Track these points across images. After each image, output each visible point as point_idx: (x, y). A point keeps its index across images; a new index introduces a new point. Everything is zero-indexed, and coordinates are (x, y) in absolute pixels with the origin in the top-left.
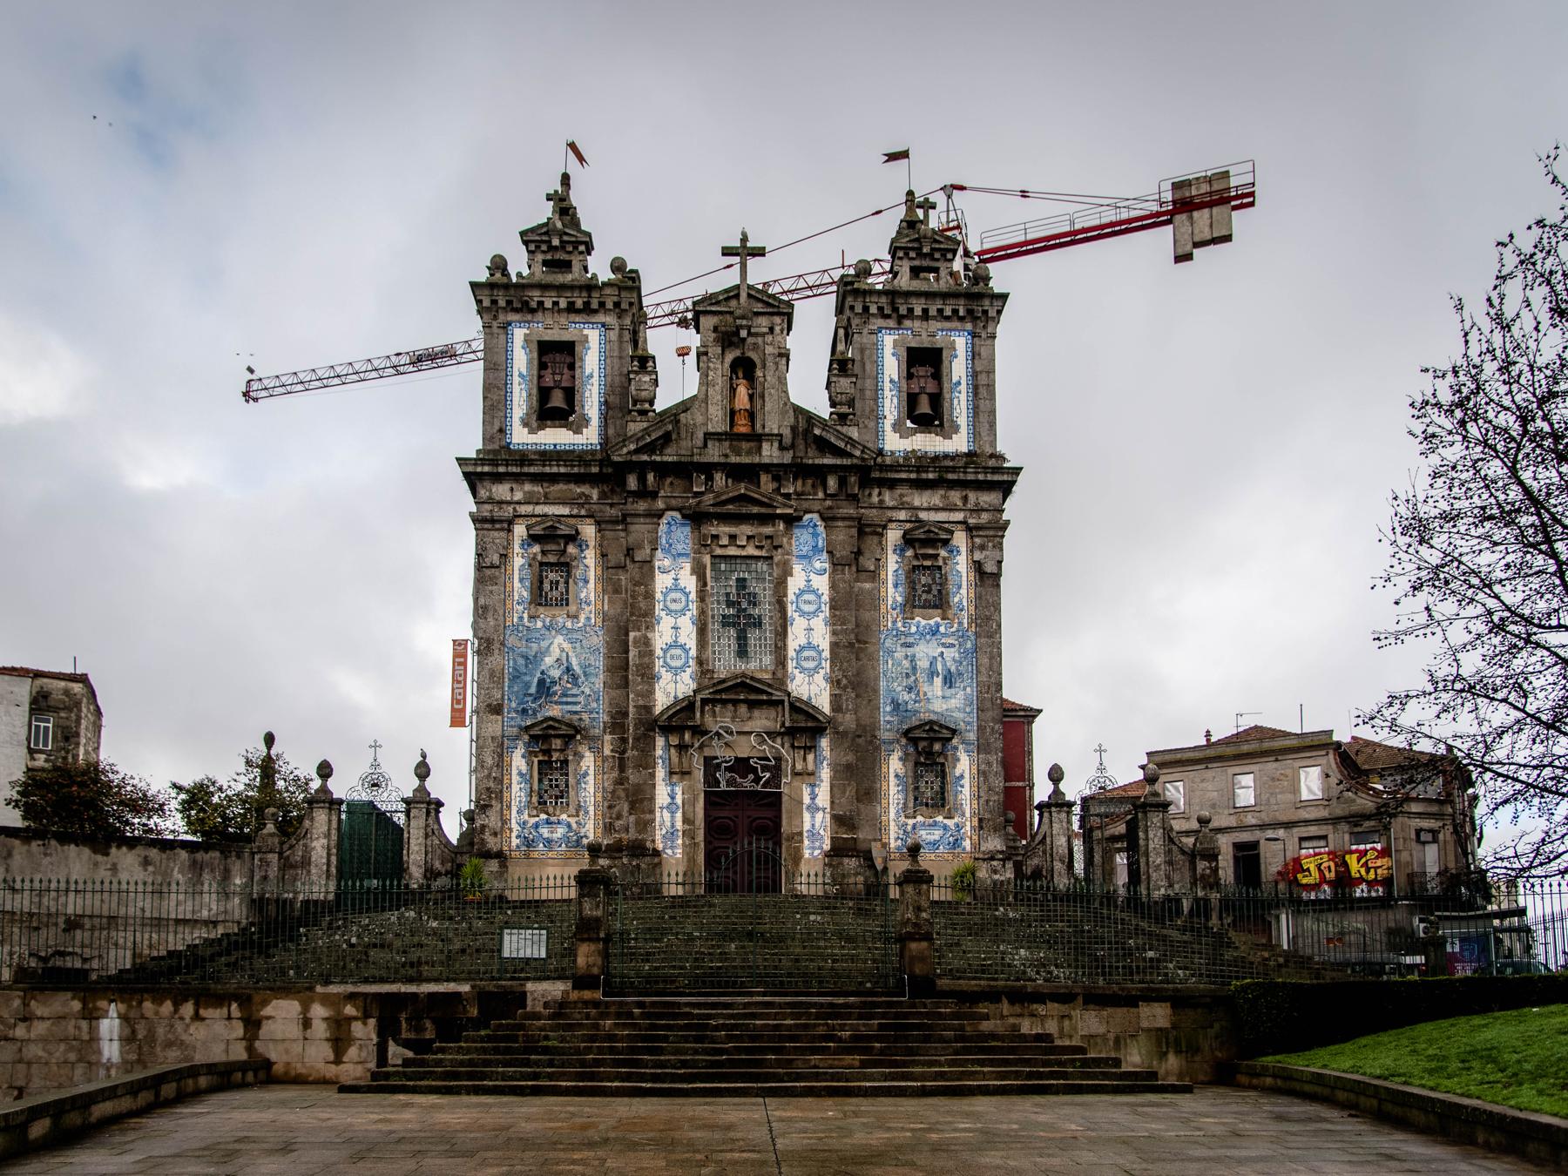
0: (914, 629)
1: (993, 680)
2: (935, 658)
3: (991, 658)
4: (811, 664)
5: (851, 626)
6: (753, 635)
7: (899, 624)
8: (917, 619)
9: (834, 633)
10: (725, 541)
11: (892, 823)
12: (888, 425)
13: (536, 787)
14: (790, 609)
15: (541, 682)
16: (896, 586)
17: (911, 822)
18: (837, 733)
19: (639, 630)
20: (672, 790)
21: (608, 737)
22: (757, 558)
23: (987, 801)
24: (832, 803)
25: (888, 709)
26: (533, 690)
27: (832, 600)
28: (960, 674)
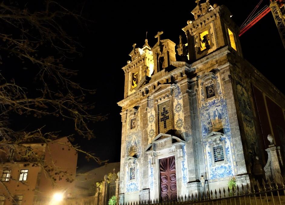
0: (208, 105)
1: (233, 112)
2: (215, 111)
3: (231, 106)
4: (180, 125)
5: (189, 110)
6: (167, 121)
7: (204, 105)
8: (209, 101)
9: (185, 114)
10: (159, 101)
11: (209, 169)
12: (196, 53)
13: (130, 175)
14: (175, 112)
15: (131, 147)
16: (202, 94)
17: (214, 168)
18: (188, 143)
19: (145, 129)
20: (152, 171)
21: (142, 158)
22: (167, 101)
23: (238, 155)
24: (188, 166)
25: (204, 131)
26: (129, 150)
27: (183, 105)
28: (223, 114)
